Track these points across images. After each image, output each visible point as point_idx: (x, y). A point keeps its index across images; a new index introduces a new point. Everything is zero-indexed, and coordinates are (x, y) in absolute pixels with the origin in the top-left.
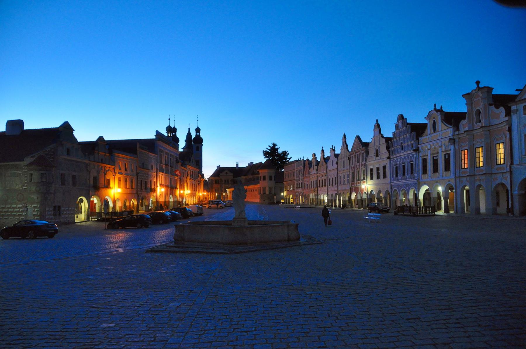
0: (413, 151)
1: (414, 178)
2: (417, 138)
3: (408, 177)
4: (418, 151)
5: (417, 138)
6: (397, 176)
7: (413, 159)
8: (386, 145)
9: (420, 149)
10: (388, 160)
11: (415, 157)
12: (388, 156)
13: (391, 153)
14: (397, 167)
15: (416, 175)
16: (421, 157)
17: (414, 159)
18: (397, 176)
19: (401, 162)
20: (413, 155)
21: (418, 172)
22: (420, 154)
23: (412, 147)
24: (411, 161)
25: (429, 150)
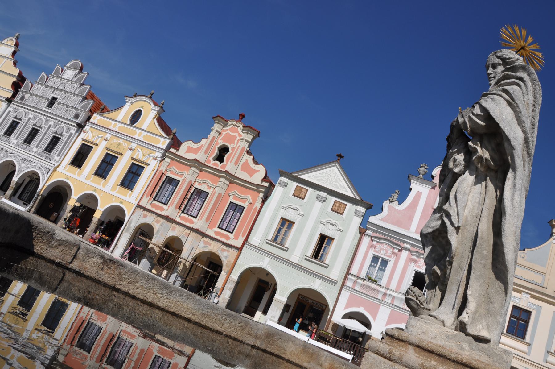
0: (76, 124)
1: (50, 159)
2: (92, 112)
3: (35, 150)
4: (81, 129)
5: (92, 112)
6: (9, 132)
7: (64, 133)
8: (15, 79)
9: (87, 128)
10: (5, 105)
11: (71, 134)
12: (9, 97)
13: (18, 98)
14: (20, 123)
15: (57, 158)
16: (83, 140)
17: (68, 135)
18: (9, 132)
19: (35, 122)
20: (69, 129)
21: (63, 156)
22: (82, 135)
23: (77, 116)
24: (59, 133)
25: (106, 140)
